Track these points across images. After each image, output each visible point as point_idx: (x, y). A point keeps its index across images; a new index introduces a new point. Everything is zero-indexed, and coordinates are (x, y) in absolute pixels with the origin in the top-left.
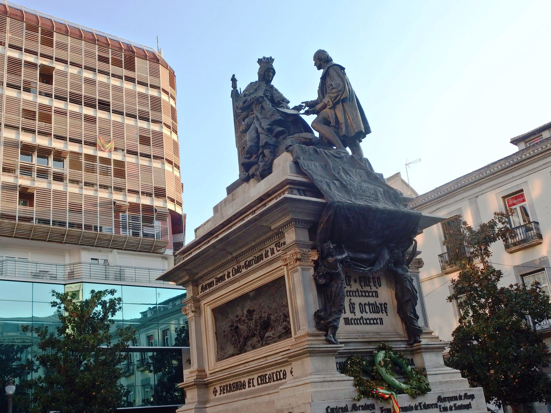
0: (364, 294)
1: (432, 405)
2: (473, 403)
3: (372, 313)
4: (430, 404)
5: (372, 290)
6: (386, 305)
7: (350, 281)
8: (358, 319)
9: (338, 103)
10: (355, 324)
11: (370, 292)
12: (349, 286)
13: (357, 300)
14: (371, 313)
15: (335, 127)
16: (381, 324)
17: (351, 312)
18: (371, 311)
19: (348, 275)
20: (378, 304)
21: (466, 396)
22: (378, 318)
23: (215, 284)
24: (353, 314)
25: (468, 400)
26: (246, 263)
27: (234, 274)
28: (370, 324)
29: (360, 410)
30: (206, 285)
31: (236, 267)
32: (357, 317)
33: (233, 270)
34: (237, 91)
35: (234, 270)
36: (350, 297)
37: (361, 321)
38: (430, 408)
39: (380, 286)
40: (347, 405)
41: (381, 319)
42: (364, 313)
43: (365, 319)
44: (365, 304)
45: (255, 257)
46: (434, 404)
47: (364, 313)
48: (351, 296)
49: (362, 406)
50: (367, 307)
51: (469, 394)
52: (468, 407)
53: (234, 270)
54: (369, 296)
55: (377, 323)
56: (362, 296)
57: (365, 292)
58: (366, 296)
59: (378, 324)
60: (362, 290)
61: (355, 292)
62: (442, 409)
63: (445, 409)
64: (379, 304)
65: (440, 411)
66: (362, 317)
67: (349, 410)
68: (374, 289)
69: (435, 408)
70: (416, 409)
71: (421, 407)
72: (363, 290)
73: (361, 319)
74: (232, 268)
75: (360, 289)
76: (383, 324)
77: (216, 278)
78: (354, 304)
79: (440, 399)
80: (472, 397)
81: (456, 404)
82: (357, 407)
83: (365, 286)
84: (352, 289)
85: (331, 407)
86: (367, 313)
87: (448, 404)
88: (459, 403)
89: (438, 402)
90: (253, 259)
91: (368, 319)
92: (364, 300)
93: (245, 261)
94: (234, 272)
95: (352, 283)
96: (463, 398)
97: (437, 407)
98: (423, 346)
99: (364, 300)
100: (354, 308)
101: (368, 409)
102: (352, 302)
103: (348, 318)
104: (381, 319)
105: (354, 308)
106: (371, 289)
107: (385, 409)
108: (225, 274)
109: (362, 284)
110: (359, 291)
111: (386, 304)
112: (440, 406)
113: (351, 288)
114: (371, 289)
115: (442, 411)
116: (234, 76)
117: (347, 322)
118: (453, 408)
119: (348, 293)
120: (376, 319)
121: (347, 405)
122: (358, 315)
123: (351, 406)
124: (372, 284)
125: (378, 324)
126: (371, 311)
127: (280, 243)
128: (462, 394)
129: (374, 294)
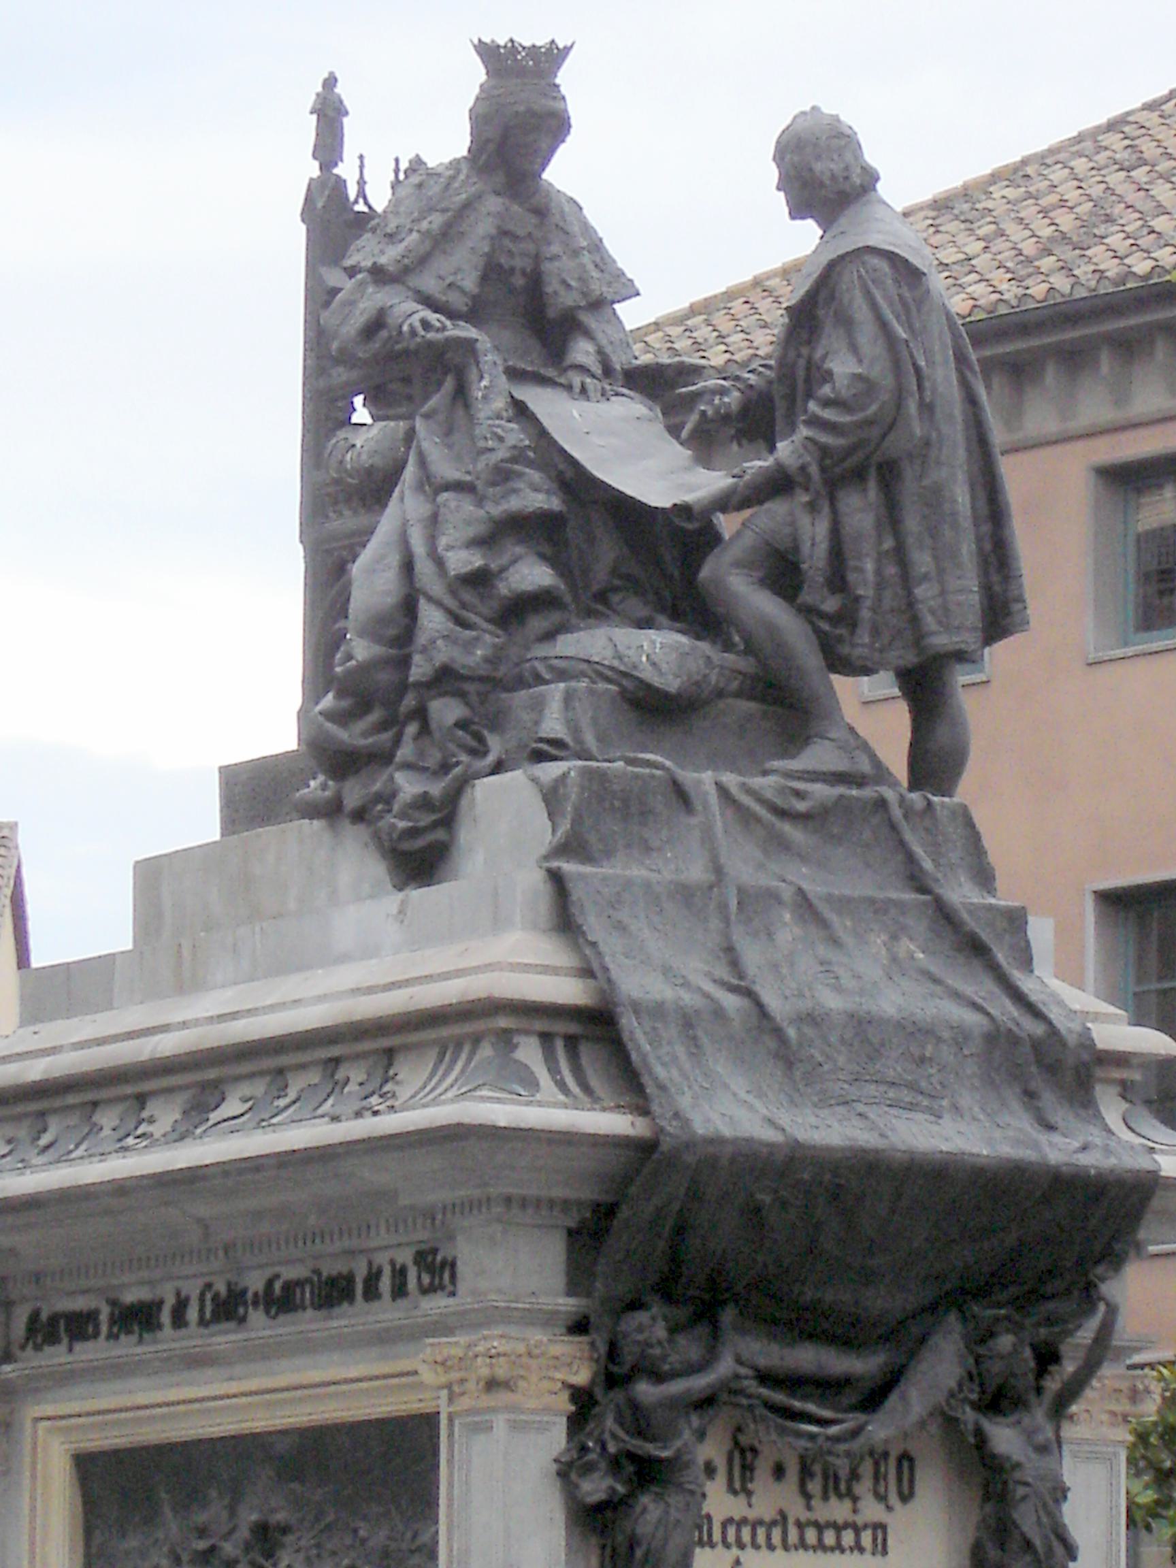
0: (811, 1535)
5: (859, 1519)
11: (846, 1526)
12: (742, 1498)
19: (744, 1440)
23: (104, 1329)
26: (270, 1283)
27: (208, 1315)
30: (54, 1319)
31: (221, 1288)
33: (202, 1295)
34: (341, 183)
35: (209, 1296)
36: (735, 1551)
39: (906, 1497)
45: (317, 1272)
53: (209, 1296)
56: (803, 1545)
57: (820, 1528)
60: (804, 1516)
74: (200, 1283)
75: (797, 1509)
77: (113, 1303)
83: (825, 1497)
84: (752, 1515)
90: (308, 1280)
93: (269, 1272)
94: (208, 1303)
95: (762, 1481)
106: (855, 1511)
108: (160, 1303)
109: (814, 1487)
110: (791, 1521)
113: (750, 1505)
116: (330, 82)
119: (731, 1531)
124: (863, 1488)
127: (439, 1258)
129: (866, 1538)
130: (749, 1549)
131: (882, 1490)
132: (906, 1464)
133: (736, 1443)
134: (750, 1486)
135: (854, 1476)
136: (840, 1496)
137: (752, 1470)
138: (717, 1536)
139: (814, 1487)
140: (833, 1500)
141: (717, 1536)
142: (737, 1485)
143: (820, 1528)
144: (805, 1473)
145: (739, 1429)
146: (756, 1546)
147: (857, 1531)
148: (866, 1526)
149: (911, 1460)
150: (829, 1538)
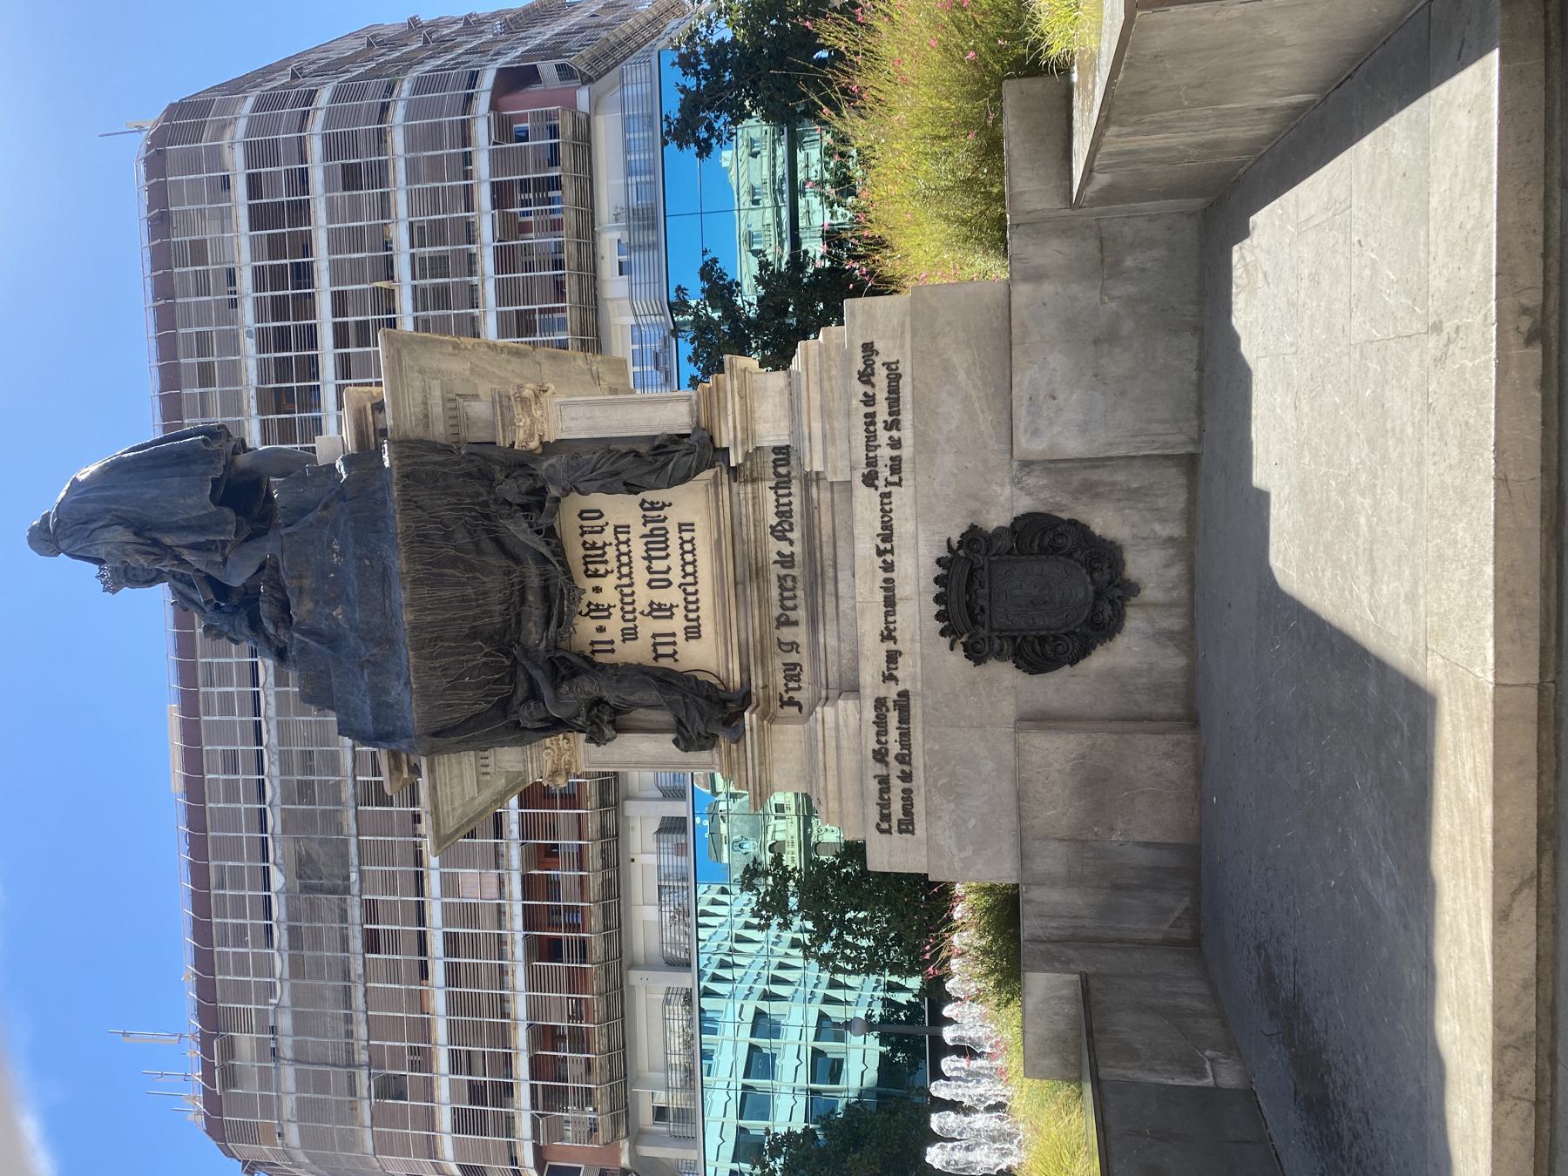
0: (625, 570)
1: (885, 513)
2: (887, 350)
3: (669, 550)
4: (882, 517)
5: (615, 542)
6: (647, 505)
7: (598, 608)
8: (685, 599)
9: (156, 543)
10: (697, 609)
11: (618, 550)
12: (611, 610)
13: (643, 596)
14: (668, 555)
15: (224, 548)
16: (693, 530)
17: (670, 617)
18: (663, 554)
19: (585, 610)
20: (646, 531)
21: (866, 377)
22: (681, 538)
24: (674, 610)
25: (876, 371)
28: (693, 563)
29: (887, 742)
32: (682, 604)
36: (637, 614)
37: (690, 589)
38: (891, 519)
39: (602, 515)
40: (875, 777)
41: (682, 527)
42: (670, 576)
43: (684, 577)
44: (649, 568)
46: (882, 504)
47: (670, 576)
48: (634, 611)
49: (878, 734)
50: (658, 565)
51: (861, 367)
52: (894, 378)
54: (628, 554)
55: (691, 541)
56: (629, 575)
57: (621, 565)
58: (629, 564)
59: (693, 538)
60: (616, 574)
61: (623, 595)
62: (895, 479)
63: (896, 466)
64: (644, 525)
65: (899, 484)
66: (680, 587)
67: (885, 773)
68: (608, 535)
69: (891, 503)
70: (888, 567)
71: (886, 551)
72: (616, 570)
73: (684, 590)
75: (612, 580)
76: (693, 524)
78: (652, 603)
79: (870, 480)
80: (869, 349)
81: (885, 422)
82: (880, 749)
83: (606, 562)
84: (619, 605)
85: (877, 818)
86: (669, 568)
87: (885, 453)
88: (882, 411)
89: (876, 489)
91: (683, 566)
92: (641, 576)
96: (870, 392)
97: (888, 495)
98: (740, 461)
99: (641, 576)
100: (660, 605)
101: (886, 717)
102: (647, 610)
103: (686, 628)
104: (680, 525)
105: (660, 607)
106: (611, 544)
107: (888, 669)
109: (602, 569)
111: (644, 501)
112: (888, 484)
114: (611, 544)
115: (901, 479)
117: (693, 633)
118: (894, 433)
119: (629, 616)
120: (684, 542)
121: (875, 777)
122: (673, 596)
123: (878, 765)
124: (599, 539)
125: (693, 538)
126: (663, 554)
128: (860, 389)
129: (623, 537)
130: (636, 605)
131: (599, 529)
132: (585, 515)
133: (587, 614)
134: (606, 606)
135: (594, 546)
136: (605, 553)
137: (597, 605)
138: (631, 625)
139: (602, 569)
140: (606, 557)
141: (631, 625)
142: (606, 613)
143: (621, 565)
144: (596, 575)
145: (580, 613)
146: (634, 602)
147: (620, 543)
148: (617, 538)
149: (583, 512)
150: (625, 559)
